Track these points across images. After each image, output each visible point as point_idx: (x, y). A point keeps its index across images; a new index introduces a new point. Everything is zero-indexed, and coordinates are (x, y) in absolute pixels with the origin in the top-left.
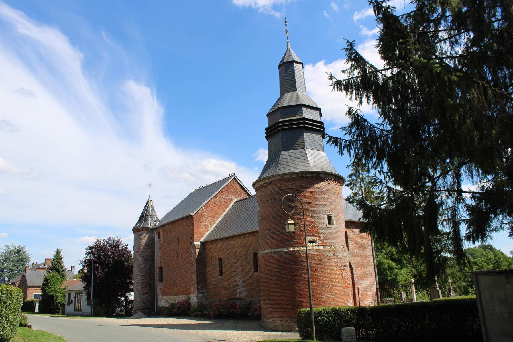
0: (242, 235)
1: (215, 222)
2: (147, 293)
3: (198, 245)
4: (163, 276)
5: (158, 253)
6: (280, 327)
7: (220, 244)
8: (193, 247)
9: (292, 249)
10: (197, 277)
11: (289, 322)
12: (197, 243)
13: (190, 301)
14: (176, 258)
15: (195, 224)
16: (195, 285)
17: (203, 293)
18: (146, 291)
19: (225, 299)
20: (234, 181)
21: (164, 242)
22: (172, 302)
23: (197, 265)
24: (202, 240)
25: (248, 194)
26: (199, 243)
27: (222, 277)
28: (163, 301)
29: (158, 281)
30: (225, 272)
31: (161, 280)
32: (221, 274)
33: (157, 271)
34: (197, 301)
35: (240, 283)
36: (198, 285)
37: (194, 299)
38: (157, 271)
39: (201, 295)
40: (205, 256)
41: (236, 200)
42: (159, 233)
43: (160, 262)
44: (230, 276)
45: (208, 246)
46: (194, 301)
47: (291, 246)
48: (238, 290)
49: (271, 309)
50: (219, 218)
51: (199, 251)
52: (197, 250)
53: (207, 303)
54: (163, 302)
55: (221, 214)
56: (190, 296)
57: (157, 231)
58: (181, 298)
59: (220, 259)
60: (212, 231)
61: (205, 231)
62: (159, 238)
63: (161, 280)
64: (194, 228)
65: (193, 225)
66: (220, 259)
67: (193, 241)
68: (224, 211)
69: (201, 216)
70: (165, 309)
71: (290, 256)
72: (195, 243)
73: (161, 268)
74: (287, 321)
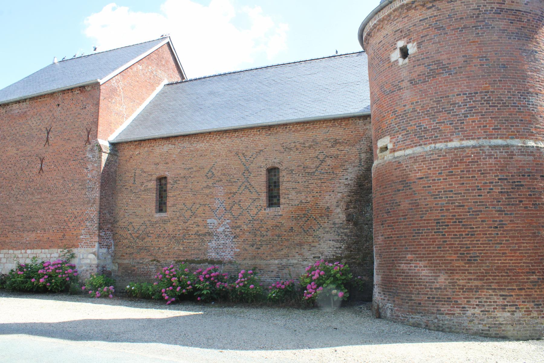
0: (235, 130)
1: (133, 111)
3: (106, 147)
6: (509, 327)
7: (166, 147)
8: (92, 150)
9: (531, 143)
10: (100, 212)
11: (535, 314)
12: (104, 143)
13: (74, 262)
14: (36, 170)
17: (108, 247)
19: (171, 261)
23: (102, 187)
24: (113, 138)
25: (183, 77)
27: (163, 215)
30: (174, 205)
32: (161, 207)
34: (95, 262)
35: (221, 229)
36: (100, 228)
37: (87, 258)
39: (104, 250)
40: (116, 171)
41: (166, 82)
45: (127, 152)
46: (88, 261)
47: (530, 135)
48: (213, 244)
49: (478, 283)
50: (140, 104)
51: (108, 159)
53: (115, 267)
55: (144, 99)
56: (75, 251)
58: (52, 255)
59: (162, 181)
60: (131, 125)
61: (116, 123)
64: (100, 111)
66: (162, 181)
67: (96, 136)
69: (114, 91)
71: (531, 158)
74: (528, 312)
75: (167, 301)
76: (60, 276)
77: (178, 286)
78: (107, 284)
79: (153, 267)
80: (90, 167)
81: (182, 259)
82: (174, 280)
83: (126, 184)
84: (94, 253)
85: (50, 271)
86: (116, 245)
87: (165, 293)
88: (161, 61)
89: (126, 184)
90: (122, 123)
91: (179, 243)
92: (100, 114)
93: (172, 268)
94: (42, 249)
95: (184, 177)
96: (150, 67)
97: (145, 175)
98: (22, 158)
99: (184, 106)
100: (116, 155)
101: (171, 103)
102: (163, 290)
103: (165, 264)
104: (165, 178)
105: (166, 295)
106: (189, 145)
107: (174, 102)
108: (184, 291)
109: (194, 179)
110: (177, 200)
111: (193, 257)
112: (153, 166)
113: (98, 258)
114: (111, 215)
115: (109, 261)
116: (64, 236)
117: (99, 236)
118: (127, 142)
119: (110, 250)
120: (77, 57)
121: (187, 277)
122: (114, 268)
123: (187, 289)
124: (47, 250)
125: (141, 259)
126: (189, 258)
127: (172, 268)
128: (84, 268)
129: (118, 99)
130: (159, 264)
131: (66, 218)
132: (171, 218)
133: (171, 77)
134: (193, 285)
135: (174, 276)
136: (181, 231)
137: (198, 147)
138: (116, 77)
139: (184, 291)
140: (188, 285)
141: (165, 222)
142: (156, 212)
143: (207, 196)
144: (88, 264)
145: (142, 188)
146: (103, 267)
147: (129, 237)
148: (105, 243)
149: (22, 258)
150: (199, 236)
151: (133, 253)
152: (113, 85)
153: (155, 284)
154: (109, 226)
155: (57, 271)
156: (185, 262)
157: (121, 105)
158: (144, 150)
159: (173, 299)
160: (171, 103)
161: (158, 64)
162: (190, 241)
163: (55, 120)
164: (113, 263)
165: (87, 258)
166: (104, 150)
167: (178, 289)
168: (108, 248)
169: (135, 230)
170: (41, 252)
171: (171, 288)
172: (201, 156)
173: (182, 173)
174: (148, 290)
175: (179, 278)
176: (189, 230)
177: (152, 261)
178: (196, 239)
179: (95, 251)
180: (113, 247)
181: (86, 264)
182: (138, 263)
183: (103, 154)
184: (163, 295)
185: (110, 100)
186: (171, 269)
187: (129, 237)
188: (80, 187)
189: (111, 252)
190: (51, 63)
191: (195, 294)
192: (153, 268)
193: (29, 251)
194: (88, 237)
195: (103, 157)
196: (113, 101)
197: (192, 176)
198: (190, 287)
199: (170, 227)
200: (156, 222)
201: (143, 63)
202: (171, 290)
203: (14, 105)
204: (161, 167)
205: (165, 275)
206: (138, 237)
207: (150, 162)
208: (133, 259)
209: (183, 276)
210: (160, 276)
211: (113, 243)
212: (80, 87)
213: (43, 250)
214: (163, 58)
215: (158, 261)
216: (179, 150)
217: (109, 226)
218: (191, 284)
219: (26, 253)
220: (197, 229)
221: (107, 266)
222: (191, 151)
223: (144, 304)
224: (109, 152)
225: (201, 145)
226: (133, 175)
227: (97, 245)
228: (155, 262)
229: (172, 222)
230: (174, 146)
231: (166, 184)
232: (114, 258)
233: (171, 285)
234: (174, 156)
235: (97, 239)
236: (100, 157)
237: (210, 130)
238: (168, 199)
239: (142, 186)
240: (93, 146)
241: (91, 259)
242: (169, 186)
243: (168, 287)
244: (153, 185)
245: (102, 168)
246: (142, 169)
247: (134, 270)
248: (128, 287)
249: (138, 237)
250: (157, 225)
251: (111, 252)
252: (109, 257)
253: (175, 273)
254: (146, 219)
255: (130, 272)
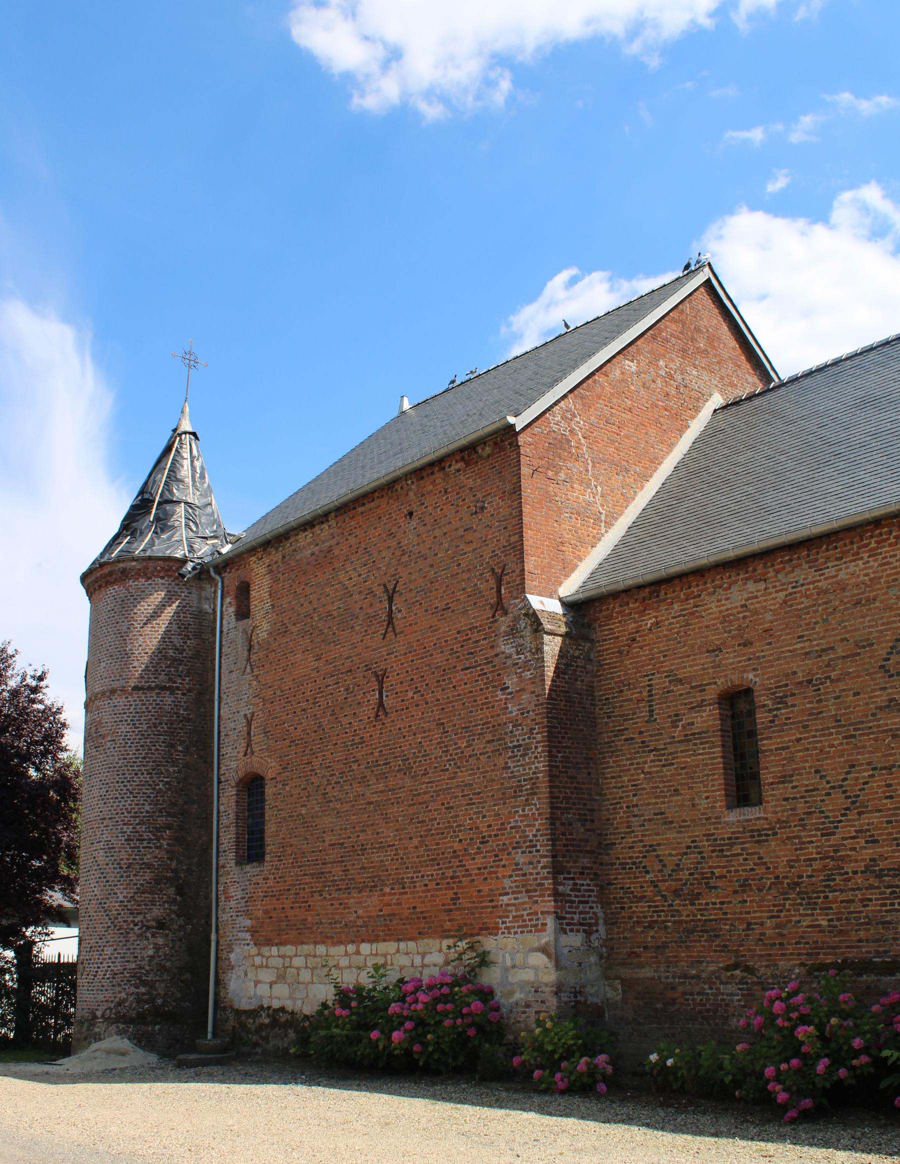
1: (628, 500)
2: (161, 925)
3: (552, 616)
4: (270, 828)
5: (235, 699)
7: (739, 593)
8: (513, 631)
10: (553, 819)
13: (491, 977)
14: (367, 712)
15: (527, 486)
16: (540, 868)
18: (157, 911)
19: (791, 966)
20: (703, 297)
21: (280, 631)
22: (365, 980)
23: (553, 739)
24: (570, 587)
26: (554, 606)
27: (752, 813)
28: (267, 976)
29: (229, 859)
30: (784, 779)
31: (252, 849)
32: (744, 787)
33: (226, 805)
34: (550, 977)
36: (557, 870)
37: (526, 964)
38: (226, 805)
39: (575, 940)
40: (591, 690)
41: (717, 400)
42: (244, 590)
43: (249, 749)
44: (839, 800)
45: (619, 626)
46: (528, 976)
50: (645, 477)
51: (562, 654)
52: (552, 647)
53: (613, 993)
54: (262, 977)
55: (656, 462)
56: (489, 943)
57: (232, 578)
58: (424, 959)
59: (737, 704)
60: (624, 543)
61: (581, 542)
62: (243, 613)
63: (252, 849)
64: (526, 509)
65: (516, 490)
66: (737, 704)
67: (521, 589)
68: (671, 446)
69: (559, 445)
70: (275, 1022)
72: (536, 602)
73: (252, 786)
75: (784, 1108)
76: (447, 1023)
77: (819, 1057)
78: (589, 1050)
79: (730, 988)
80: (511, 682)
81: (829, 960)
82: (804, 1033)
83: (626, 724)
84: (544, 950)
85: (420, 1006)
86: (611, 922)
87: (778, 1081)
88: (693, 340)
89: (626, 724)
90: (597, 539)
91: (812, 905)
92: (526, 519)
93: (795, 993)
94: (399, 940)
95: (810, 682)
96: (661, 363)
97: (679, 689)
98: (329, 681)
99: (782, 458)
100: (587, 639)
101: (741, 459)
102: (769, 1071)
103: (773, 976)
104: (748, 692)
105: (778, 1088)
106: (812, 575)
107: (750, 454)
108: (843, 1072)
109: (841, 685)
110: (791, 760)
111: (866, 950)
112: (705, 659)
113: (558, 966)
114: (588, 825)
115: (592, 974)
116: (455, 899)
117: (556, 894)
118: (615, 595)
119: (593, 937)
120: (458, 382)
121: (850, 1023)
122: (610, 994)
123: (854, 1068)
124: (411, 945)
125: (691, 965)
126: (852, 954)
127: (795, 993)
128: (518, 996)
129: (576, 468)
130: (751, 979)
131: (456, 846)
132: (779, 821)
133: (732, 385)
134: (874, 1052)
135: (804, 1020)
136: (816, 865)
137: (842, 575)
138: (562, 404)
139: (843, 1072)
140: (856, 1054)
141: (759, 836)
142: (729, 807)
143: (894, 736)
144: (528, 983)
145: (677, 733)
146: (576, 994)
147: (649, 892)
148: (576, 917)
149: (350, 967)
150: (880, 875)
151: (665, 946)
152: (555, 428)
153: (739, 1048)
154: (586, 861)
155: (440, 1007)
156: (839, 968)
157: (589, 485)
158: (669, 612)
159: (807, 1103)
160: (741, 459)
161: (684, 351)
162: (850, 895)
163: (405, 558)
164: (607, 978)
165: (525, 967)
166: (548, 626)
167: (821, 1067)
168: (588, 933)
169: (667, 871)
170: (398, 951)
171: (795, 1062)
172: (858, 602)
173: (801, 668)
174: (721, 1067)
175: (820, 1027)
176: (843, 859)
177: (727, 968)
178: (871, 887)
179: (547, 943)
180: (602, 929)
181: (523, 985)
182: (685, 976)
183: (546, 638)
184: (769, 1087)
185: (550, 473)
186: (790, 995)
187: (649, 892)
188: (490, 748)
189: (596, 944)
190: (396, 414)
191: (883, 1085)
192: (731, 992)
193: (365, 948)
194: (523, 898)
195: (546, 648)
196: (562, 476)
197: (833, 675)
198: (864, 1059)
199: (778, 853)
200: (732, 841)
201: (639, 352)
202: (798, 1071)
203: (302, 535)
204: (729, 658)
205: (773, 1017)
206: (677, 893)
207: (692, 647)
208: (669, 963)
209: (834, 1021)
210: (757, 1021)
211: (601, 915)
212: (462, 450)
213: (402, 945)
214: (698, 330)
215: (748, 970)
216: (782, 595)
217: (586, 861)
218: (866, 1050)
219: (358, 953)
220: (869, 852)
221: (589, 990)
222: (821, 592)
223: (704, 1119)
224: (563, 629)
225: (851, 570)
226: (645, 694)
227: (550, 921)
228: (738, 972)
229: (782, 833)
230: (762, 585)
231: (751, 713)
232: (609, 960)
233: (797, 1053)
234: (769, 617)
235: (550, 905)
236: (539, 650)
237: (876, 513)
238: (763, 761)
239: (674, 725)
240: (516, 619)
241: (536, 969)
242: (761, 717)
243: (787, 1061)
244: (708, 718)
245: (548, 682)
246: (670, 674)
247: (673, 1002)
248: (654, 1057)
249: (677, 893)
250: (737, 849)
251: (596, 944)
252: (593, 959)
253: (806, 1010)
254: (698, 832)
255: (659, 1006)
